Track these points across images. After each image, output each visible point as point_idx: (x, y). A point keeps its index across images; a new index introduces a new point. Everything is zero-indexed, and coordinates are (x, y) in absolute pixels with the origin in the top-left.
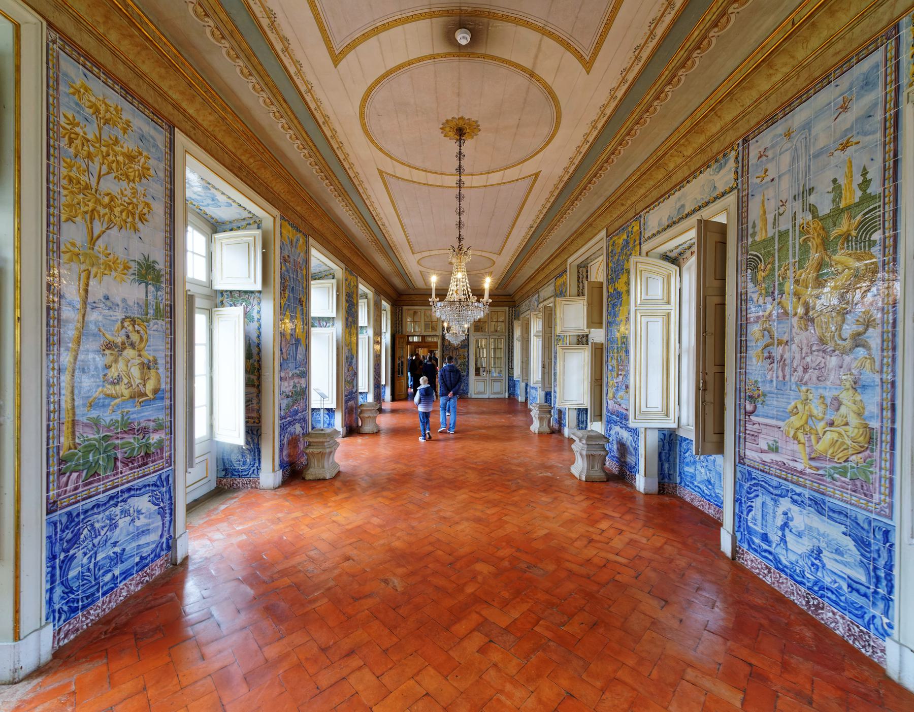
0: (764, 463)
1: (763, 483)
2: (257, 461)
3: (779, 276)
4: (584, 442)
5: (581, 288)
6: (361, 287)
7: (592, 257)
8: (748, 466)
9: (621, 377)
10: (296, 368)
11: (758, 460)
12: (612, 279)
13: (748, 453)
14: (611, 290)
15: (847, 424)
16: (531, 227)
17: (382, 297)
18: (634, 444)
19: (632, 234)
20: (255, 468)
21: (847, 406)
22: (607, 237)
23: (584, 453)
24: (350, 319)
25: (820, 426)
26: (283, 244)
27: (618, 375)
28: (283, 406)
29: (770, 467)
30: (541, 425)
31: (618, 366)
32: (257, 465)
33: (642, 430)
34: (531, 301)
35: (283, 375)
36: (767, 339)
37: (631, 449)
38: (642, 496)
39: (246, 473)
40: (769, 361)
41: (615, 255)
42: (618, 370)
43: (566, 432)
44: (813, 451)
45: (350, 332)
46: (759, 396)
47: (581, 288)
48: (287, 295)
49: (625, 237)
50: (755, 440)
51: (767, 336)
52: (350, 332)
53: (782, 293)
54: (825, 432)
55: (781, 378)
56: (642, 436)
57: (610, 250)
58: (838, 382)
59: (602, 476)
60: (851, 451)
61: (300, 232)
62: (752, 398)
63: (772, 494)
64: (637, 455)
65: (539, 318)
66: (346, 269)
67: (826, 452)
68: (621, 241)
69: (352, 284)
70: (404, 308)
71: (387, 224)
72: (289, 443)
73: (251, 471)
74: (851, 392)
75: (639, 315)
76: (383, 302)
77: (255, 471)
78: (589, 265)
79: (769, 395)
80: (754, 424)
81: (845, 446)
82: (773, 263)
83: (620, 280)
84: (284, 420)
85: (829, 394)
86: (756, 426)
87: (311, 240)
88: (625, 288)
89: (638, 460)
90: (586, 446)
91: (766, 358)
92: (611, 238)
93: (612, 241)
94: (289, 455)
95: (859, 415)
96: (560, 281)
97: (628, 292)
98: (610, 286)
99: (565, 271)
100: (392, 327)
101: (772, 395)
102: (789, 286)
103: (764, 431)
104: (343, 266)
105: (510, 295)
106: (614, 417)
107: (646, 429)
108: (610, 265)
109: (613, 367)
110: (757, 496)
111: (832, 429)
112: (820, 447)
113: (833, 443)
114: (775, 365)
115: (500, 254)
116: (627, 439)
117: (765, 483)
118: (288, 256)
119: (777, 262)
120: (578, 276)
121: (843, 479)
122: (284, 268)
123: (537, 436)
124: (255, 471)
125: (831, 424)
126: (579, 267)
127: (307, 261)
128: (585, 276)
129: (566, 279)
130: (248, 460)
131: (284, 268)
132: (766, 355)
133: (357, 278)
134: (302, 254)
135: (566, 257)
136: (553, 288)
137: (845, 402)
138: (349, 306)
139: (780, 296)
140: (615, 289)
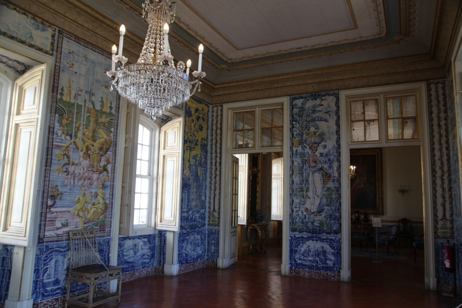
0: (58, 235)
1: (57, 249)
3: (75, 127)
8: (46, 242)
11: (54, 235)
13: (47, 234)
15: (99, 203)
21: (100, 196)
25: (90, 206)
29: (62, 236)
36: (66, 160)
40: (66, 173)
44: (86, 219)
46: (58, 195)
50: (53, 223)
51: (66, 159)
53: (76, 136)
54: (91, 209)
55: (72, 184)
58: (97, 185)
60: (100, 214)
62: (53, 197)
63: (62, 252)
67: (91, 217)
74: (101, 189)
79: (64, 194)
80: (53, 213)
81: (98, 213)
82: (73, 118)
85: (94, 191)
86: (54, 214)
91: (65, 172)
95: (103, 199)
101: (67, 194)
102: (80, 134)
103: (60, 216)
110: (52, 259)
111: (95, 206)
112: (89, 216)
113: (94, 212)
114: (69, 176)
117: (58, 247)
119: (75, 119)
121: (97, 227)
125: (94, 205)
132: (65, 169)
137: (99, 194)
139: (75, 138)
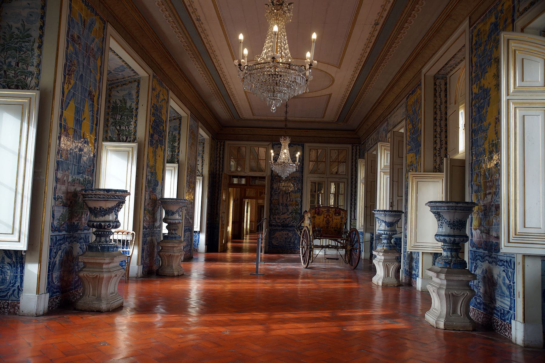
2: (19, 280)
4: (443, 276)
5: (439, 103)
6: (172, 103)
7: (452, 62)
9: (489, 197)
10: (79, 173)
12: (477, 76)
14: (475, 90)
16: (377, 24)
17: (200, 124)
18: (507, 282)
19: (502, 13)
20: (16, 288)
22: (470, 27)
23: (443, 292)
24: (156, 136)
26: (73, 20)
27: (485, 195)
28: (57, 215)
30: (387, 274)
31: (485, 183)
32: (18, 284)
33: (519, 259)
34: (378, 133)
35: (60, 175)
37: (504, 289)
38: (519, 350)
39: (5, 294)
41: (480, 45)
42: (486, 187)
43: (419, 284)
45: (155, 153)
47: (439, 103)
48: (72, 82)
49: (493, 20)
52: (155, 153)
56: (519, 269)
57: (474, 42)
59: (467, 323)
61: (97, 14)
64: (512, 295)
65: (387, 150)
66: (154, 76)
68: (487, 27)
69: (161, 96)
70: (227, 142)
71: (202, 18)
72: (62, 263)
73: (11, 292)
75: (512, 107)
76: (201, 132)
77: (16, 292)
78: (448, 77)
83: (487, 75)
84: (57, 233)
87: (110, 29)
88: (494, 83)
89: (513, 301)
90: (445, 282)
92: (475, 27)
93: (476, 31)
94: (61, 279)
96: (413, 99)
97: (498, 86)
98: (474, 86)
99: (420, 85)
100: (210, 164)
104: (150, 71)
105: (354, 130)
106: (481, 250)
107: (524, 256)
108: (474, 59)
109: (479, 186)
115: (339, 67)
116: (499, 276)
118: (79, 37)
120: (435, 89)
122: (71, 48)
123: (380, 289)
124: (16, 292)
126: (435, 78)
127: (102, 50)
128: (443, 89)
129: (420, 94)
130: (8, 278)
131: (71, 48)
133: (168, 92)
134: (96, 40)
135: (420, 67)
136: (404, 110)
138: (155, 121)
140: (480, 88)
